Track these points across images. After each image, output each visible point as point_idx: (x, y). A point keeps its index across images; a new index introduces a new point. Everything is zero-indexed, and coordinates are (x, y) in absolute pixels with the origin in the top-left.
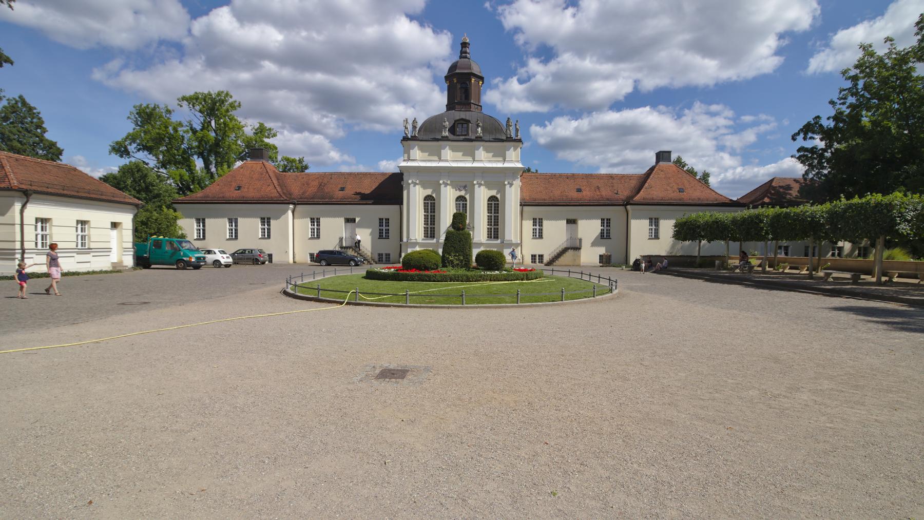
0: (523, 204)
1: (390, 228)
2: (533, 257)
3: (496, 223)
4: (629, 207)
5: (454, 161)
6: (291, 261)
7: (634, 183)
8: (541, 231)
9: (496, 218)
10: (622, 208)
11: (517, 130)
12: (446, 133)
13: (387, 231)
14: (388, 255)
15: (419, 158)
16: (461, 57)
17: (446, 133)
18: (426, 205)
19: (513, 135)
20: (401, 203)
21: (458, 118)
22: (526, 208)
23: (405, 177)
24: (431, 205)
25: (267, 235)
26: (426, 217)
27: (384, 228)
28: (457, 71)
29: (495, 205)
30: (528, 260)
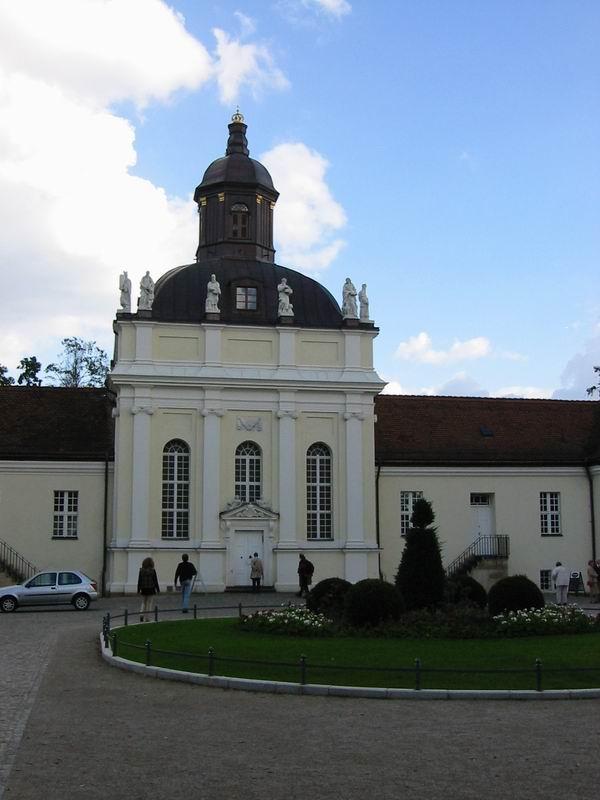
9: (327, 493)
11: (365, 304)
18: (167, 463)
22: (384, 469)
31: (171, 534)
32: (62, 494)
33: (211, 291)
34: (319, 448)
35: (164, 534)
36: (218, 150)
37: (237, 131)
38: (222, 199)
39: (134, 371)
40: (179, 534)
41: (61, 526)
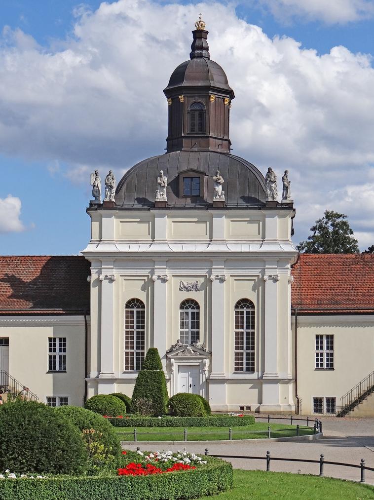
1: (67, 354)
2: (318, 402)
3: (251, 345)
5: (176, 242)
8: (331, 356)
9: (251, 336)
11: (286, 188)
12: (161, 196)
13: (63, 359)
15: (119, 233)
16: (192, 56)
17: (161, 196)
19: (279, 199)
20: (87, 312)
24: (137, 312)
27: (57, 354)
29: (246, 312)
30: (308, 407)
31: (242, 369)
32: (55, 339)
33: (160, 184)
34: (244, 303)
35: (236, 369)
36: (183, 54)
38: (182, 100)
39: (103, 248)
40: (247, 369)
41: (55, 362)
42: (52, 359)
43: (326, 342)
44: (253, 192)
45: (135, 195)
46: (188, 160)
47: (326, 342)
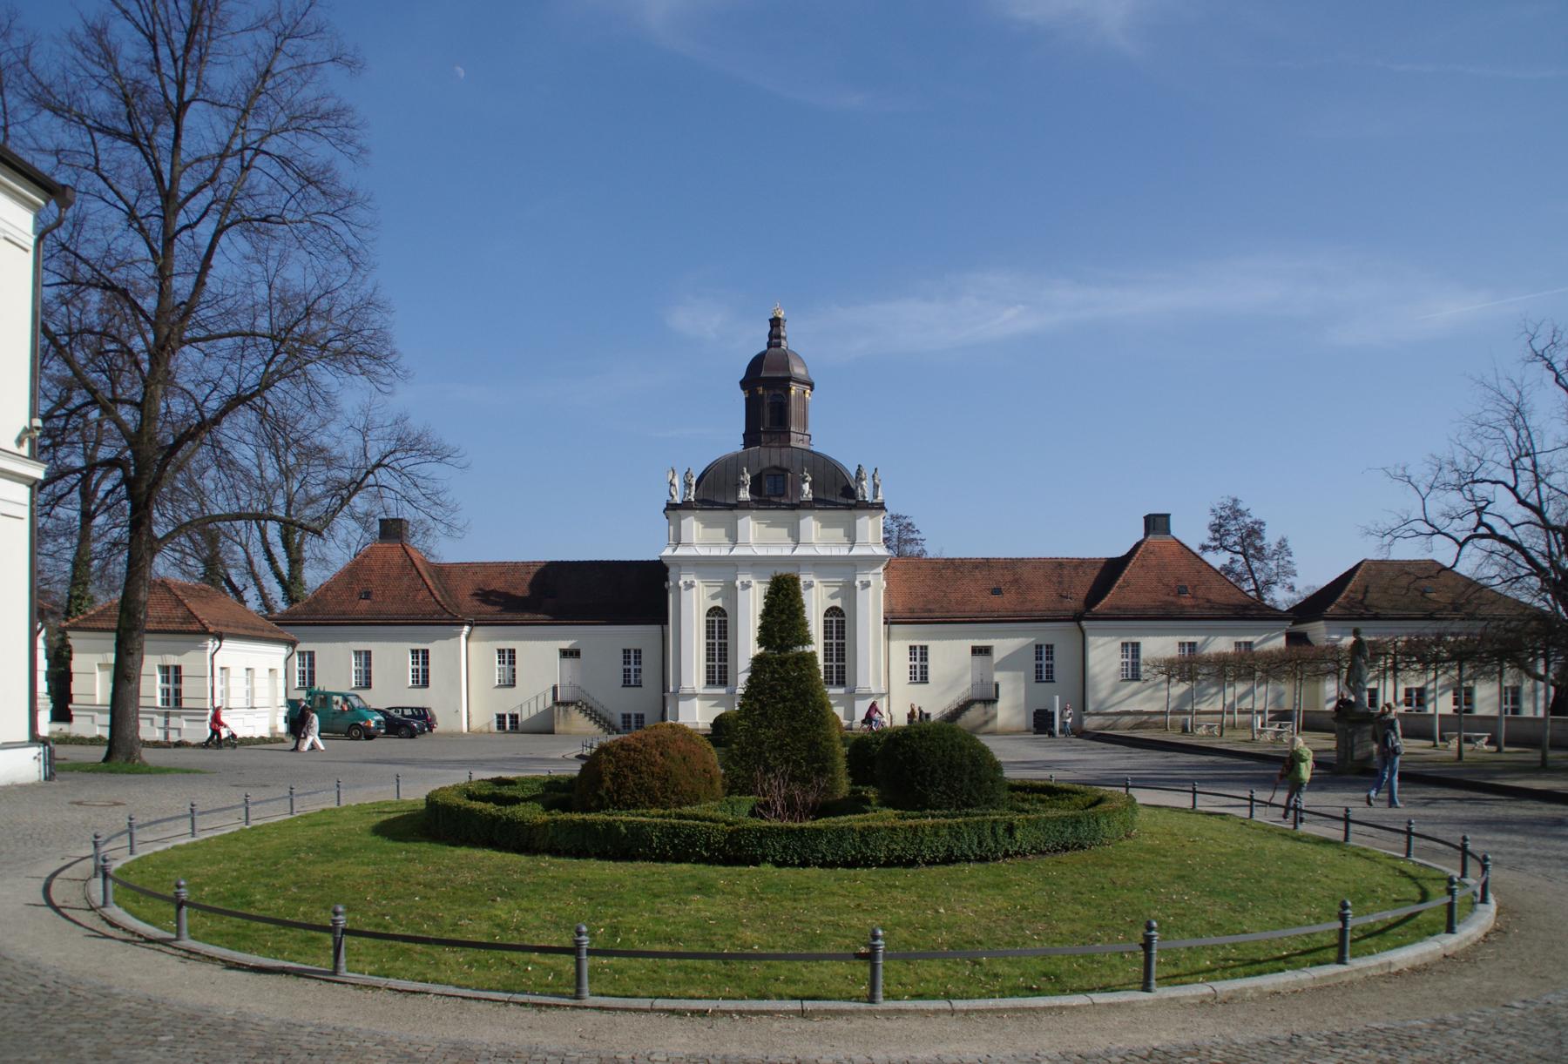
0: (890, 620)
1: (643, 667)
4: (1084, 623)
6: (465, 729)
7: (1089, 578)
9: (841, 649)
10: (1072, 625)
11: (876, 486)
12: (745, 495)
14: (640, 717)
15: (700, 537)
16: (769, 345)
19: (869, 498)
20: (667, 623)
21: (766, 464)
22: (895, 628)
23: (671, 574)
24: (720, 623)
25: (422, 680)
26: (710, 648)
28: (763, 374)
37: (775, 323)
39: (680, 552)
42: (626, 672)
43: (920, 654)
44: (840, 494)
45: (713, 493)
46: (769, 456)
47: (920, 654)
